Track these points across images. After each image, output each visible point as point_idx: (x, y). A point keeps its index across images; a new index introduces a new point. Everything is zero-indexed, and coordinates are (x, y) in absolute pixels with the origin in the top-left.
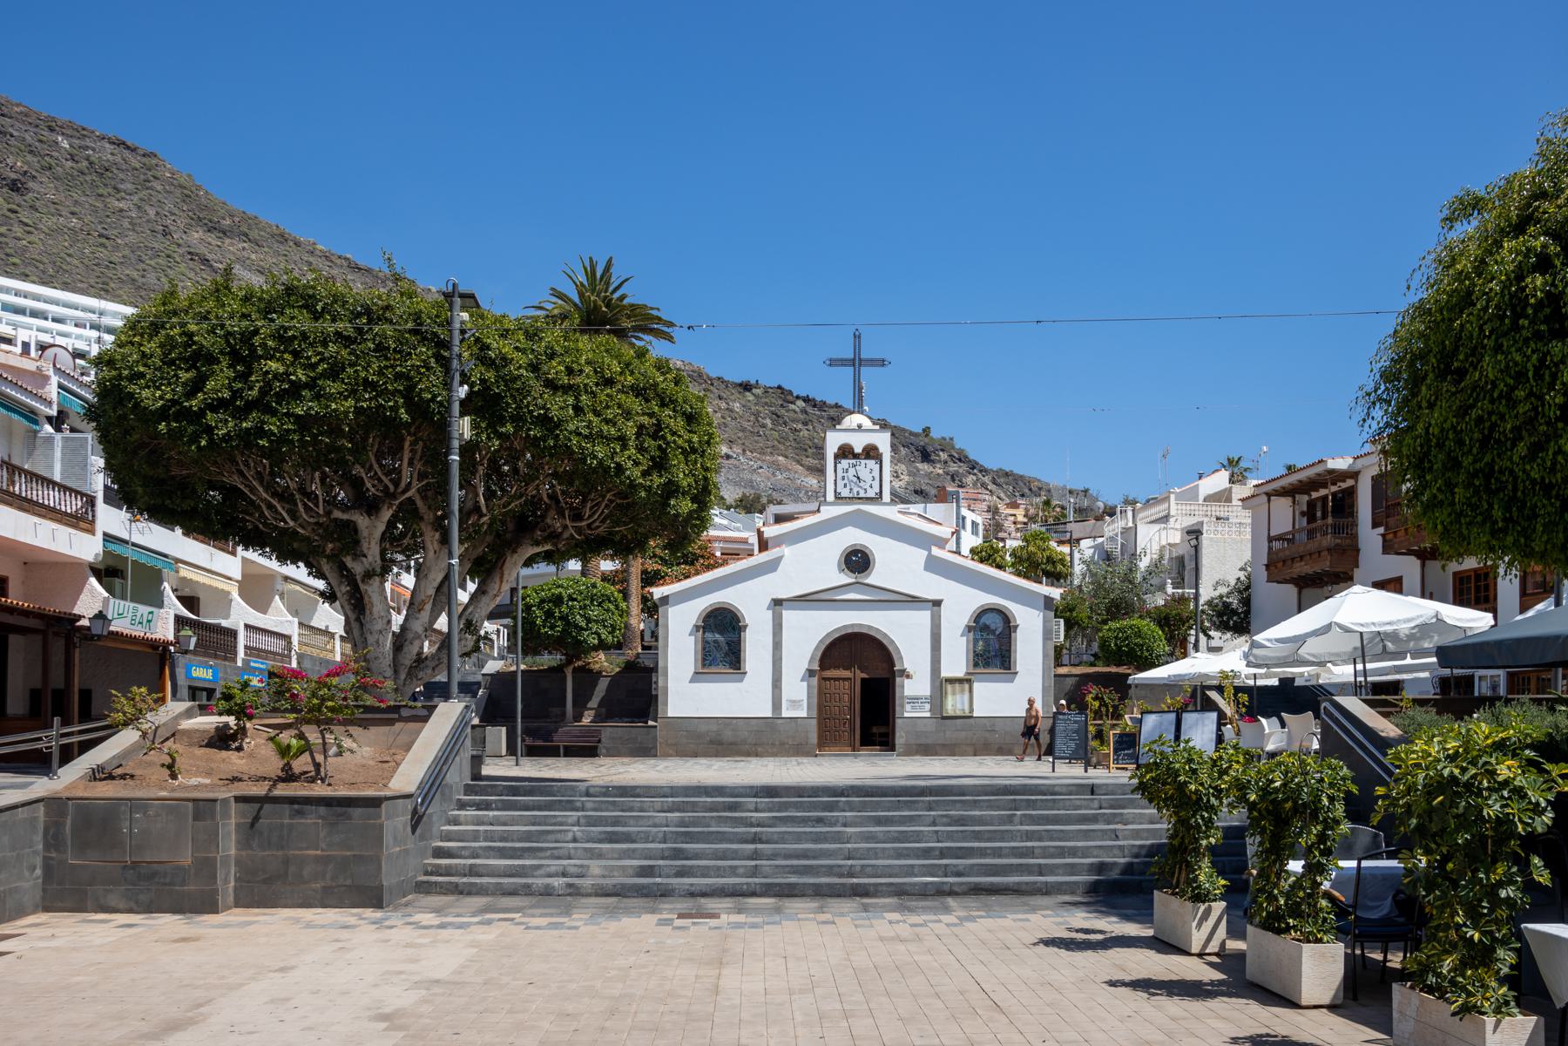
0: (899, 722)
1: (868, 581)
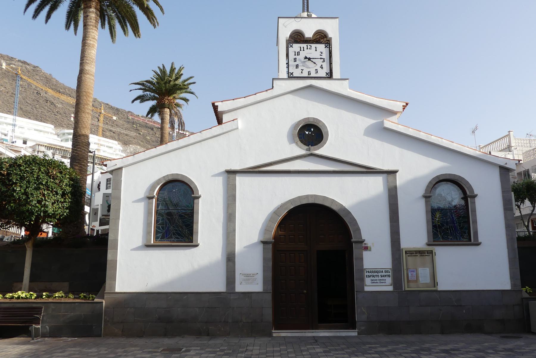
0: (358, 297)
1: (321, 151)
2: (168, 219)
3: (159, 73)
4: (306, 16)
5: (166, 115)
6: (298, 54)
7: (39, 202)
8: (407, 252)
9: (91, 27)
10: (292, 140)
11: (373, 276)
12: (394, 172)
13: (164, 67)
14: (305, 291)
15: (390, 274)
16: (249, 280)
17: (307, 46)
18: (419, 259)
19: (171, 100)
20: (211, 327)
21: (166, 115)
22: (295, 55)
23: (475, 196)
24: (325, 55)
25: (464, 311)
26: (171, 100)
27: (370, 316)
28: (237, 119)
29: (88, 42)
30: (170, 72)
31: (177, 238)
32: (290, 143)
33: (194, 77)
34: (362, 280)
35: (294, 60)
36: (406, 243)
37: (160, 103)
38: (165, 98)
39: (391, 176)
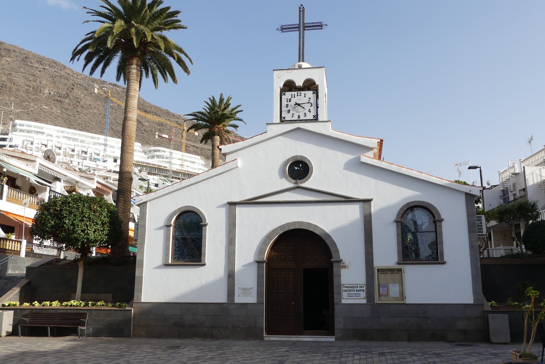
0: (337, 308)
2: (183, 243)
3: (210, 103)
4: (298, 68)
5: (217, 142)
6: (290, 100)
7: (83, 231)
8: (379, 270)
9: (133, 81)
10: (282, 174)
11: (350, 291)
12: (369, 201)
13: (213, 98)
14: (293, 303)
15: (364, 289)
16: (246, 293)
17: (298, 93)
18: (389, 275)
19: (221, 127)
20: (214, 332)
21: (217, 142)
22: (287, 102)
23: (442, 220)
24: (313, 101)
25: (429, 322)
26: (221, 127)
27: (346, 325)
28: (237, 159)
29: (130, 93)
30: (220, 103)
31: (190, 258)
32: (281, 178)
33: (241, 105)
34: (340, 294)
35: (286, 106)
36: (379, 262)
37: (211, 131)
38: (215, 126)
39: (366, 204)
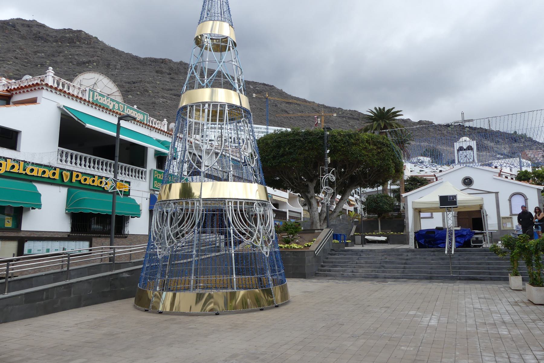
18: (507, 219)
23: (527, 199)
36: (502, 215)
